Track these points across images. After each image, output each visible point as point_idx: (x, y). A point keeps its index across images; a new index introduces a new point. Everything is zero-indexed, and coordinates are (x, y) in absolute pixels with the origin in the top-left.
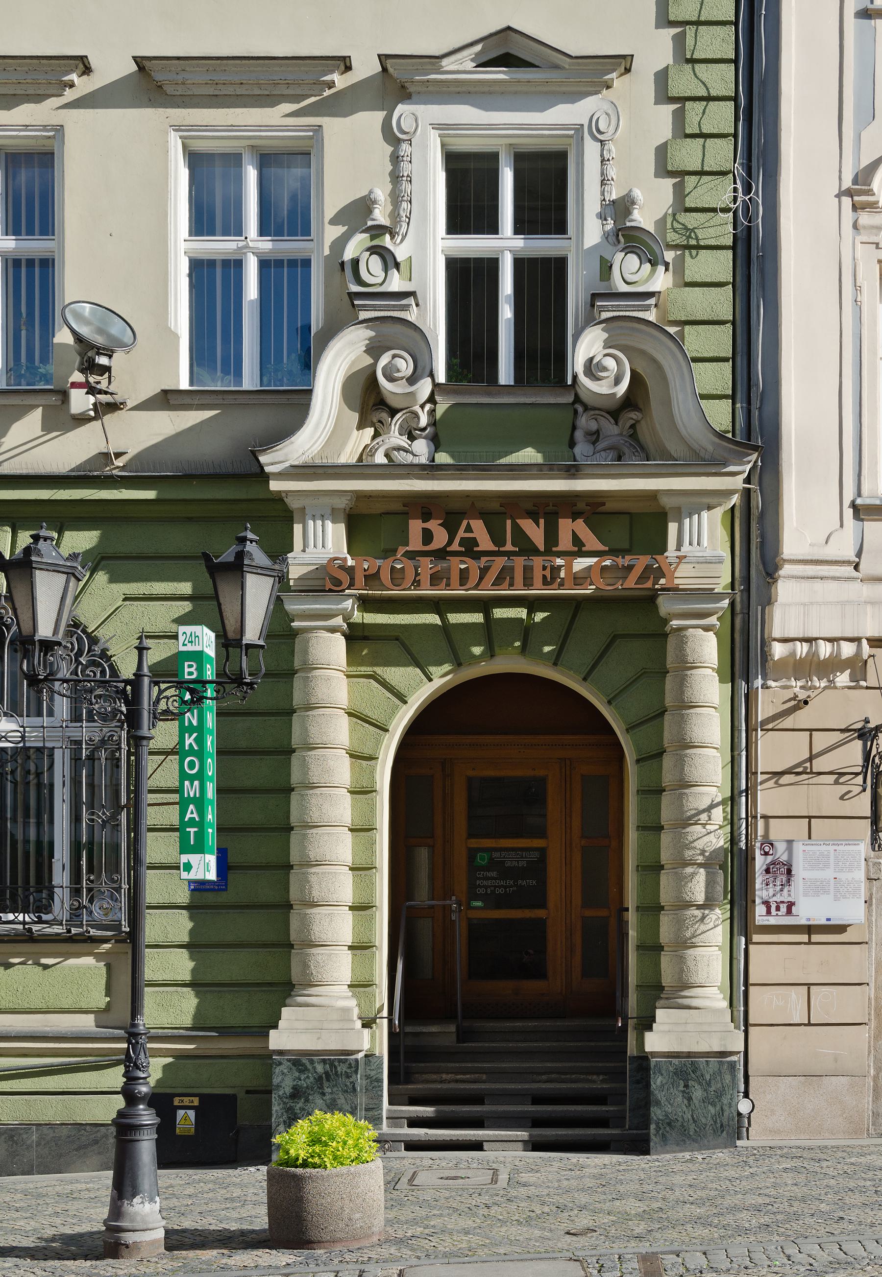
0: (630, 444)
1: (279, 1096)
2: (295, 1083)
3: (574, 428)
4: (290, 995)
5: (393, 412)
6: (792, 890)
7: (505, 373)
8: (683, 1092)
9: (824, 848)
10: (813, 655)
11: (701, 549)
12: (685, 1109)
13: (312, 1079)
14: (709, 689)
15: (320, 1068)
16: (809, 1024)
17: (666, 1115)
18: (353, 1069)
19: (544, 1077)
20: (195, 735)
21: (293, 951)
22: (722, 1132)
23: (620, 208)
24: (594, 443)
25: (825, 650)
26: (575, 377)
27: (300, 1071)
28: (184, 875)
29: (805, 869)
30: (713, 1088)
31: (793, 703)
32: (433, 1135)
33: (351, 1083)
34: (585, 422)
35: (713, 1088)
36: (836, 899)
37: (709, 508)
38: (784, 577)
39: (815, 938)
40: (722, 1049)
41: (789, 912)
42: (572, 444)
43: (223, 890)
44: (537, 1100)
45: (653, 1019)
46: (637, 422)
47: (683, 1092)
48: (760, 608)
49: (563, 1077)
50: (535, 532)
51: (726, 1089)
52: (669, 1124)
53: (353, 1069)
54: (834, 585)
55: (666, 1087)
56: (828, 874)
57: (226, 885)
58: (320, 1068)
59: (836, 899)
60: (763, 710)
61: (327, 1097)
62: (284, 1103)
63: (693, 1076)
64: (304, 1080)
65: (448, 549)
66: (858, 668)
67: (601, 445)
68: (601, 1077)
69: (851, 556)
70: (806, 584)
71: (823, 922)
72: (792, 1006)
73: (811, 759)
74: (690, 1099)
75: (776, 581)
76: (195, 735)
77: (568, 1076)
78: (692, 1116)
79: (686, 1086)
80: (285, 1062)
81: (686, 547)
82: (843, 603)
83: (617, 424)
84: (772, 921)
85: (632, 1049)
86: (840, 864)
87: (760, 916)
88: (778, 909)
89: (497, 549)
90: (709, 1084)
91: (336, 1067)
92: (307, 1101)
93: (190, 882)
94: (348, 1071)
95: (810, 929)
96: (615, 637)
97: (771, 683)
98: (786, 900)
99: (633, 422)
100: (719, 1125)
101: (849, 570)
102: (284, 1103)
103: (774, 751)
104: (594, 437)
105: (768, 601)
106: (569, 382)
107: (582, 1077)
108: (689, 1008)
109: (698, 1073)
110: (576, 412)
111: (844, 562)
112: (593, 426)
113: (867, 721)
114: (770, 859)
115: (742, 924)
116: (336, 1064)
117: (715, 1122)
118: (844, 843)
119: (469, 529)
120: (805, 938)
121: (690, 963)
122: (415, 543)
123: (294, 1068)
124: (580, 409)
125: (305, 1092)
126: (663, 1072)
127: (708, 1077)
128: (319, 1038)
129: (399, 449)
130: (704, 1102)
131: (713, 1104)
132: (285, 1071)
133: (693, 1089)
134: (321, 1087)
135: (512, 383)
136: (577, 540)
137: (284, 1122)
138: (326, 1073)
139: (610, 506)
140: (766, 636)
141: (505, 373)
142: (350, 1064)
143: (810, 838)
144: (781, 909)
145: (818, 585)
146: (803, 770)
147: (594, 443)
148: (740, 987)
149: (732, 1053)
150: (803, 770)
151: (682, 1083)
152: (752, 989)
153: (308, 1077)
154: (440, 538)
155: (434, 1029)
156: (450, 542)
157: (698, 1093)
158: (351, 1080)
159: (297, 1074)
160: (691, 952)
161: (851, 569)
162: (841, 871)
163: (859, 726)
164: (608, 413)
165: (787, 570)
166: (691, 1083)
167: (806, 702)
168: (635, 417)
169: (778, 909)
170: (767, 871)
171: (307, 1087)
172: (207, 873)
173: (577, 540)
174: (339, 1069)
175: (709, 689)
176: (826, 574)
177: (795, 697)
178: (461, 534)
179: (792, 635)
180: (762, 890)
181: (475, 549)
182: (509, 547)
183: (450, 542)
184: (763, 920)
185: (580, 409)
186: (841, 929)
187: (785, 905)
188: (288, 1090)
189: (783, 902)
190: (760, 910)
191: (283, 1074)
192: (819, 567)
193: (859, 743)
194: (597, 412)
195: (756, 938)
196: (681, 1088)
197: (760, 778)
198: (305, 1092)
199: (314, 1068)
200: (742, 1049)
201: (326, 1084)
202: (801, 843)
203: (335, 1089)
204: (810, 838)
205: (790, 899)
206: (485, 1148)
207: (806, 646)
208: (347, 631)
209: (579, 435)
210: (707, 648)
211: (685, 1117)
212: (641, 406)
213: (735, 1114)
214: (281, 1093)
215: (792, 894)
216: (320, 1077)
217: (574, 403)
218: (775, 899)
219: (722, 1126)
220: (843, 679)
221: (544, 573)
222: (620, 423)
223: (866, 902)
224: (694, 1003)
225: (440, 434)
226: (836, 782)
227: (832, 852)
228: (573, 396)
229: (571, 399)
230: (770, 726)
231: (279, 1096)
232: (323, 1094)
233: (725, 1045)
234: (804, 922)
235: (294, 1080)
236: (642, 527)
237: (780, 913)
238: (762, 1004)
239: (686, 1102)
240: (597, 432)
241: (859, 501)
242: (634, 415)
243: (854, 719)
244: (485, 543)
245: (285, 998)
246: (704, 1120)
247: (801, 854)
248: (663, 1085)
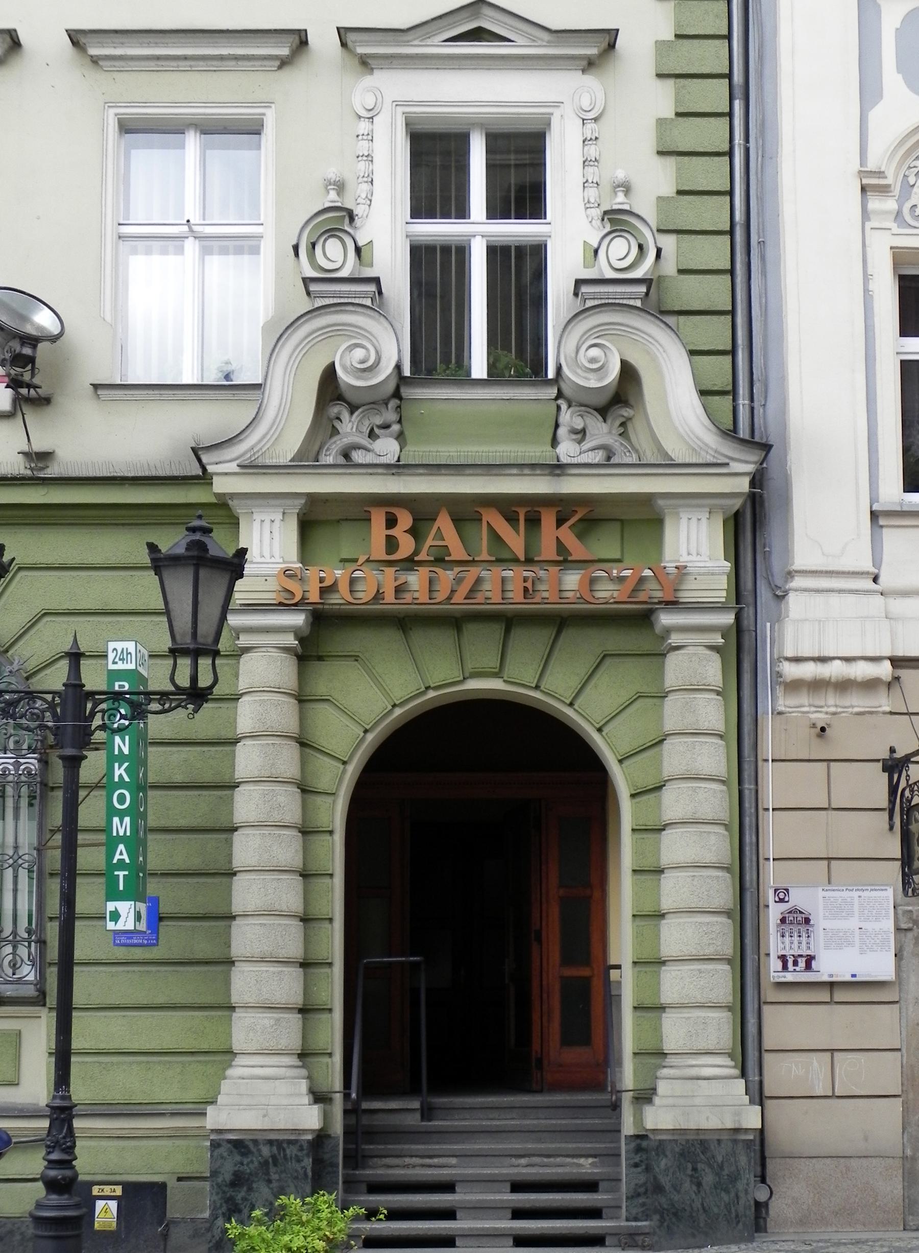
0: (622, 444)
1: (217, 1184)
2: (236, 1168)
3: (557, 426)
4: (230, 1066)
5: (353, 409)
6: (812, 943)
7: (479, 368)
8: (692, 1176)
9: (846, 894)
12: (694, 1196)
13: (256, 1163)
15: (266, 1151)
17: (673, 1205)
18: (305, 1152)
19: (523, 1161)
20: (126, 764)
21: (234, 1014)
22: (738, 1222)
24: (579, 442)
26: (559, 369)
27: (243, 1155)
28: (111, 926)
29: (825, 918)
30: (726, 1172)
32: (396, 1229)
33: (303, 1167)
34: (568, 418)
35: (726, 1172)
36: (862, 952)
38: (796, 590)
39: (839, 996)
40: (737, 1126)
41: (808, 967)
42: (554, 442)
43: (154, 945)
44: (517, 1187)
45: (654, 1090)
46: (629, 419)
47: (692, 1176)
48: (768, 624)
49: (545, 1160)
50: (515, 541)
51: (742, 1172)
52: (675, 1214)
53: (305, 1152)
54: (852, 598)
55: (671, 1171)
56: (853, 924)
57: (157, 939)
58: (266, 1151)
59: (862, 952)
61: (275, 1185)
62: (224, 1192)
63: (702, 1156)
64: (248, 1165)
65: (416, 559)
67: (587, 445)
68: (590, 1160)
71: (848, 978)
76: (126, 764)
77: (552, 1160)
78: (702, 1204)
79: (695, 1169)
80: (224, 1144)
83: (605, 421)
84: (789, 977)
85: (628, 1127)
86: (866, 912)
88: (795, 963)
89: (471, 558)
90: (721, 1167)
91: (284, 1150)
92: (250, 1189)
93: (116, 933)
94: (299, 1154)
95: (832, 985)
96: (605, 656)
98: (804, 954)
99: (623, 420)
100: (733, 1215)
101: (869, 584)
102: (224, 1192)
104: (581, 434)
105: (778, 619)
106: (551, 374)
107: (569, 1160)
109: (709, 1154)
110: (559, 408)
111: (862, 573)
112: (579, 424)
113: (892, 750)
114: (784, 907)
116: (285, 1145)
117: (730, 1212)
118: (869, 888)
119: (439, 535)
120: (824, 996)
122: (378, 550)
123: (235, 1151)
124: (564, 406)
125: (248, 1180)
126: (668, 1153)
127: (720, 1159)
128: (264, 1116)
129: (358, 447)
130: (716, 1188)
132: (225, 1154)
133: (703, 1173)
134: (268, 1173)
135: (485, 376)
136: (561, 547)
137: (223, 1214)
138: (274, 1157)
141: (479, 368)
142: (301, 1146)
143: (829, 883)
144: (800, 965)
145: (834, 599)
147: (579, 442)
149: (747, 1130)
151: (690, 1166)
152: (767, 1057)
153: (252, 1162)
154: (407, 545)
155: (393, 1105)
156: (416, 552)
157: (708, 1179)
158: (303, 1164)
159: (238, 1158)
163: (886, 755)
166: (700, 1166)
168: (625, 414)
169: (795, 963)
170: (783, 920)
171: (251, 1174)
172: (137, 923)
173: (561, 547)
174: (288, 1152)
178: (429, 542)
179: (806, 654)
180: (776, 944)
181: (447, 558)
182: (485, 556)
183: (416, 552)
184: (779, 977)
185: (564, 406)
187: (804, 959)
188: (228, 1177)
189: (801, 956)
191: (222, 1157)
194: (583, 408)
196: (689, 1172)
198: (248, 1180)
199: (259, 1151)
200: (760, 1127)
201: (272, 1170)
202: (820, 889)
203: (283, 1175)
204: (829, 883)
205: (809, 952)
206: (457, 1243)
208: (300, 650)
209: (562, 432)
211: (694, 1205)
212: (632, 401)
213: (752, 1203)
214: (220, 1180)
215: (812, 947)
216: (266, 1163)
217: (556, 399)
218: (792, 952)
219: (737, 1216)
221: (525, 584)
222: (609, 421)
223: (896, 955)
225: (406, 433)
227: (856, 901)
228: (556, 391)
231: (217, 1184)
232: (269, 1181)
233: (739, 1121)
234: (825, 978)
235: (236, 1165)
237: (798, 969)
238: (781, 1073)
239: (694, 1188)
244: (458, 552)
245: (225, 1069)
246: (716, 1210)
247: (821, 899)
248: (667, 1169)
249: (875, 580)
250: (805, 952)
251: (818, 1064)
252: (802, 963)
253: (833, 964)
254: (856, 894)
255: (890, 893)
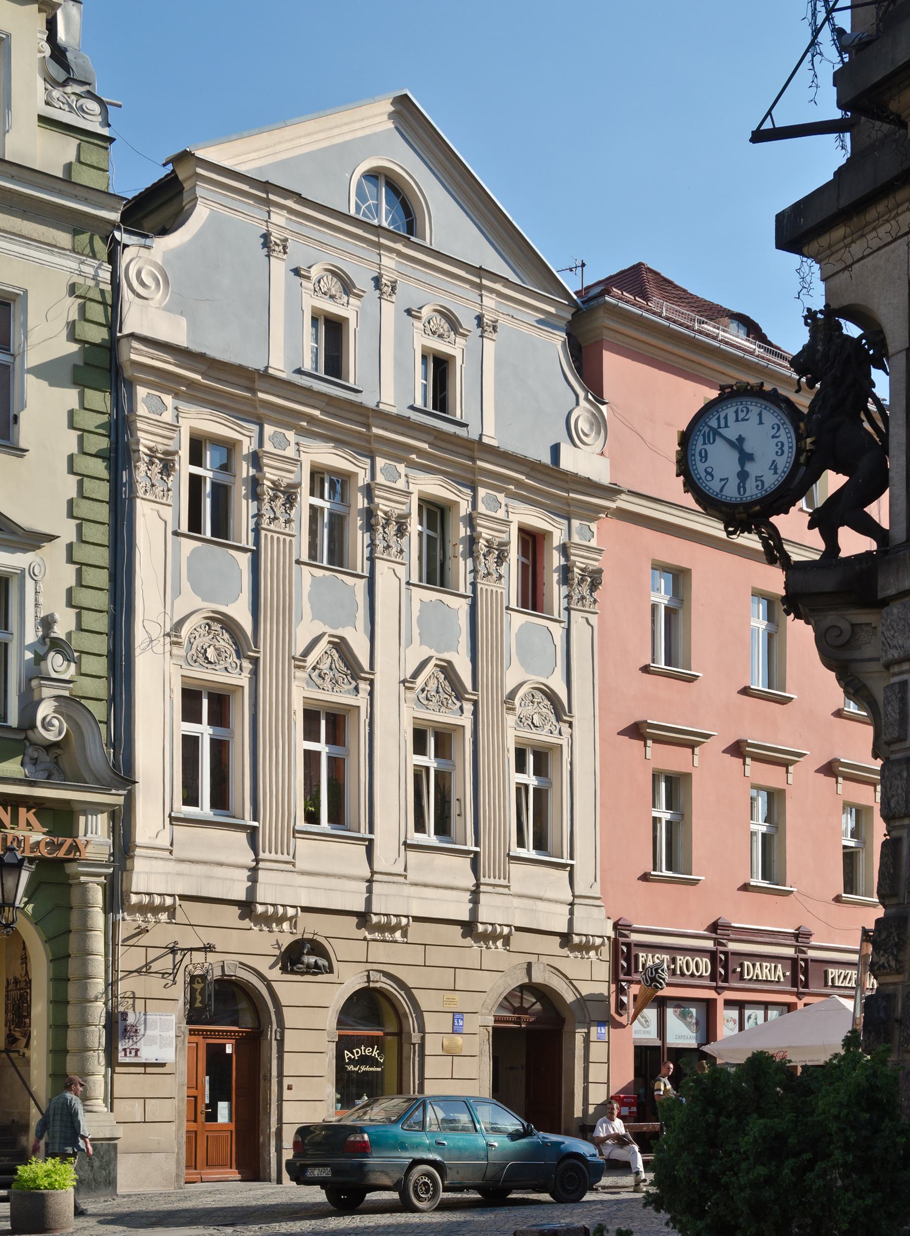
10: (151, 903)
11: (95, 835)
14: (98, 918)
16: (145, 1122)
23: (47, 623)
25: (157, 900)
31: (138, 930)
36: (161, 1047)
37: (102, 812)
39: (149, 1070)
41: (136, 1055)
54: (161, 863)
59: (161, 1047)
60: (122, 934)
66: (171, 911)
69: (167, 844)
70: (148, 861)
72: (135, 1110)
73: (146, 965)
74: (92, 1167)
75: (132, 857)
81: (89, 835)
82: (168, 874)
84: (127, 1060)
87: (121, 1058)
95: (145, 1065)
97: (127, 918)
101: (166, 854)
103: (129, 959)
108: (91, 1112)
115: (111, 1061)
120: (142, 1070)
121: (91, 1085)
131: (105, 1170)
139: (47, 805)
140: (124, 889)
145: (154, 862)
146: (145, 970)
148: (111, 1100)
150: (145, 970)
152: (115, 1100)
160: (91, 1078)
161: (168, 853)
162: (163, 1031)
164: (43, 747)
165: (138, 851)
167: (148, 931)
175: (98, 918)
176: (155, 856)
177: (139, 927)
186: (163, 1065)
190: (121, 1054)
192: (156, 852)
193: (171, 956)
195: (118, 1069)
197: (121, 975)
207: (147, 898)
210: (97, 896)
220: (163, 917)
224: (95, 1109)
226: (163, 977)
229: (23, 737)
230: (130, 942)
236: (61, 818)
240: (36, 759)
241: (173, 814)
242: (59, 751)
243: (168, 941)
249: (171, 852)
250: (134, 1047)
251: (138, 1104)
252: (133, 1052)
253: (148, 1054)
254: (158, 1017)
255: (174, 1017)
